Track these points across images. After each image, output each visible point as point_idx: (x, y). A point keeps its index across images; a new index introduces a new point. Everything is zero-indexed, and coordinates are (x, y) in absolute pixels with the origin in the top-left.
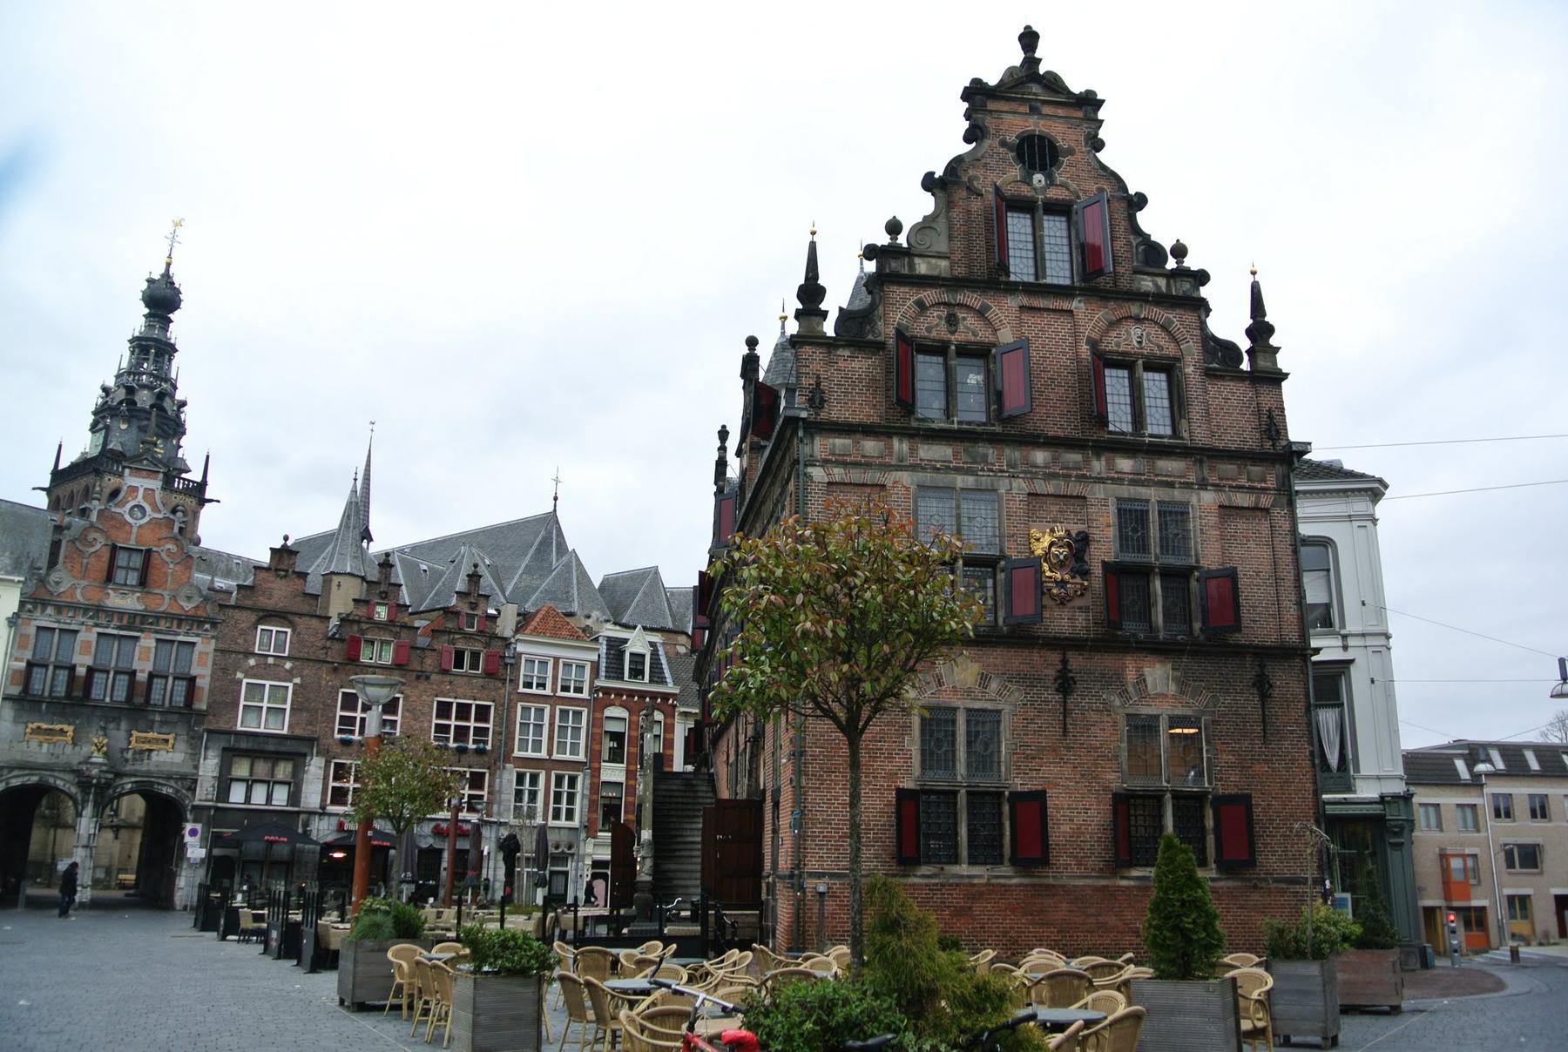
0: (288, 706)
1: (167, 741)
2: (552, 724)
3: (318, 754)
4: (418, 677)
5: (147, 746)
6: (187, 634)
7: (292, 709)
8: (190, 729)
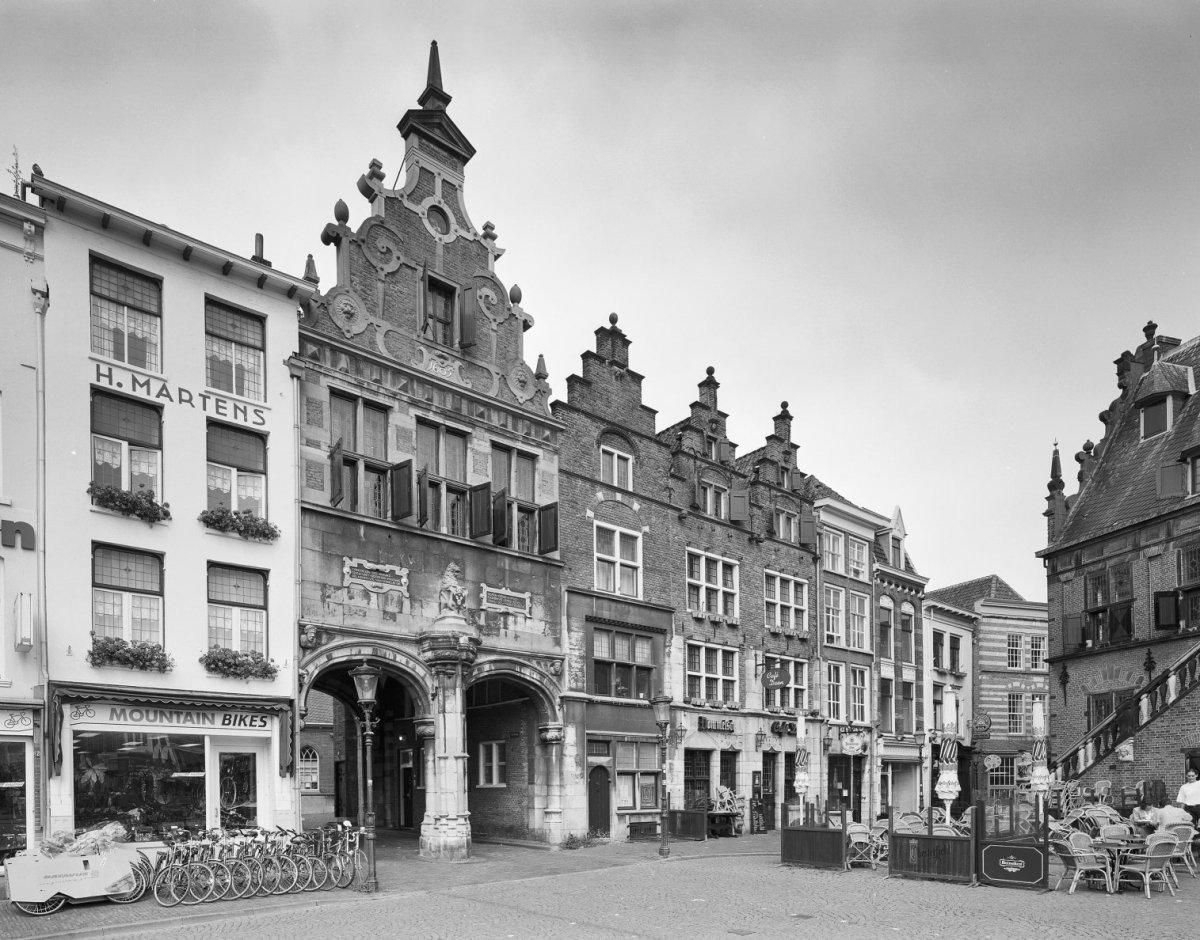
0: (639, 563)
1: (522, 601)
2: (847, 611)
3: (677, 634)
4: (750, 540)
5: (503, 609)
6: (526, 440)
7: (645, 568)
8: (546, 587)
